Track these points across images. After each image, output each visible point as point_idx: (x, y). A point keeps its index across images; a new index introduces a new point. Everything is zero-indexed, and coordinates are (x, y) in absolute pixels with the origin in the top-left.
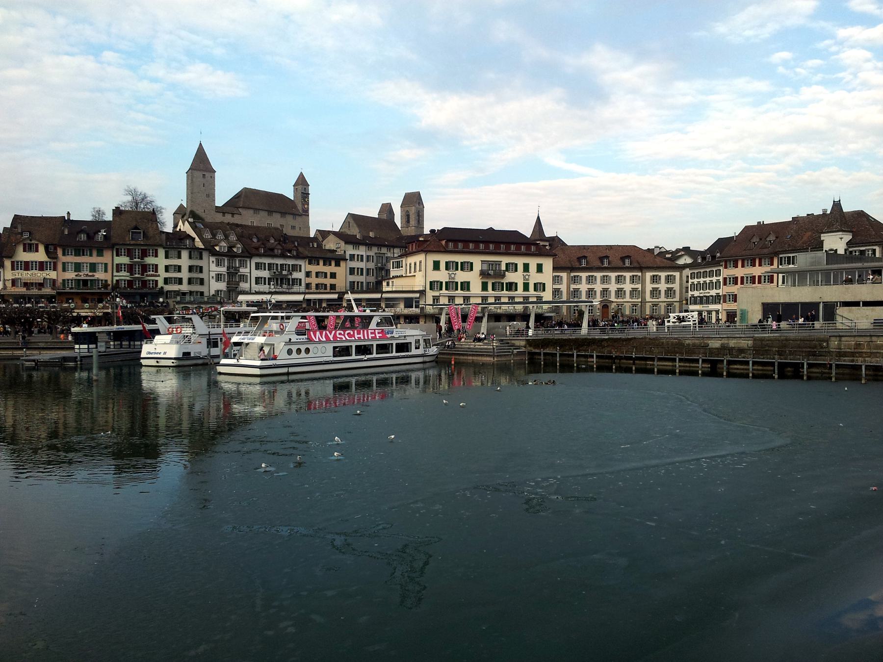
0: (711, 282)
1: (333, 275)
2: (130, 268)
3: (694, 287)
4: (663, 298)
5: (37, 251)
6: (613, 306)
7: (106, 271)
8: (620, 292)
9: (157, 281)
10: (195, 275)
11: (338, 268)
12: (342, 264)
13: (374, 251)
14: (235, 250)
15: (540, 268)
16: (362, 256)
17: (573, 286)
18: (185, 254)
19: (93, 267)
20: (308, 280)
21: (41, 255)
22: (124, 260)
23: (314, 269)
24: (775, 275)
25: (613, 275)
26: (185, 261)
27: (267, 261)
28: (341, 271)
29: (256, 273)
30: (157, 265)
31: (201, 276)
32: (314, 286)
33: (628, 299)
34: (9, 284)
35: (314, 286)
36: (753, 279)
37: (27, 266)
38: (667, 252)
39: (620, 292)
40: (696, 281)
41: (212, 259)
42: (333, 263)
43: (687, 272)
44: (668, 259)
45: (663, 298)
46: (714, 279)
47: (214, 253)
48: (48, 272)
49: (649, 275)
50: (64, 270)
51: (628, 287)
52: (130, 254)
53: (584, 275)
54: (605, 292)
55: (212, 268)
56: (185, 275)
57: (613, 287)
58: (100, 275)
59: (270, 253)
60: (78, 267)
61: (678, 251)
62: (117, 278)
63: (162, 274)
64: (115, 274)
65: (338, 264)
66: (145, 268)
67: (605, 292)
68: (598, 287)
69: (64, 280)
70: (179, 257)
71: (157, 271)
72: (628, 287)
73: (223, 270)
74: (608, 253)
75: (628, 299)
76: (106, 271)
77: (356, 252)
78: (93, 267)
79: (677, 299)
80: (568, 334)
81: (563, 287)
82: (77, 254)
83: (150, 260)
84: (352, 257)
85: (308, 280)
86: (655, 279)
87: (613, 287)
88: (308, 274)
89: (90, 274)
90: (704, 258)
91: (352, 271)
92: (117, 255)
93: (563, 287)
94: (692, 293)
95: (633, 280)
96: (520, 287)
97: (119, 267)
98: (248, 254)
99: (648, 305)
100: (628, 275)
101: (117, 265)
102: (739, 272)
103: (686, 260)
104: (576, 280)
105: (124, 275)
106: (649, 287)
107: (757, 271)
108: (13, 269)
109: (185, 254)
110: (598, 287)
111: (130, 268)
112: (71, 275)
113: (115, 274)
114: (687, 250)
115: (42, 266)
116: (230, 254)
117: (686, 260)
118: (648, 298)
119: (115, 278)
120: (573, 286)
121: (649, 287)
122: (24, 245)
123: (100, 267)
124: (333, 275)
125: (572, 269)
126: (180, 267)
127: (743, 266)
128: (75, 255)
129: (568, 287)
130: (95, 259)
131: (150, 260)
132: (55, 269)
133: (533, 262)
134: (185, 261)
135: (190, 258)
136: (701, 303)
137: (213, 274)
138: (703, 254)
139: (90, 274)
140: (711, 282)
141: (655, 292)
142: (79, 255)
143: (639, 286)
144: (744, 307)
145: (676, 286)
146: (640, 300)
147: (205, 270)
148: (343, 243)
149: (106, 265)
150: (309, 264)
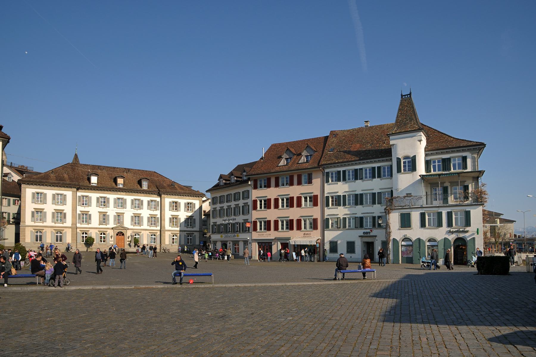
6: (129, 233)
8: (137, 219)
17: (80, 209)
25: (129, 198)
33: (145, 225)
49: (168, 200)
51: (145, 213)
53: (94, 196)
54: (119, 217)
57: (128, 213)
67: (119, 217)
68: (112, 211)
72: (145, 213)
75: (145, 225)
79: (197, 228)
81: (68, 209)
87: (128, 213)
93: (68, 209)
94: (214, 220)
100: (145, 199)
110: (112, 211)
118: (167, 225)
120: (80, 209)
121: (168, 214)
129: (74, 209)
136: (226, 231)
146: (159, 228)
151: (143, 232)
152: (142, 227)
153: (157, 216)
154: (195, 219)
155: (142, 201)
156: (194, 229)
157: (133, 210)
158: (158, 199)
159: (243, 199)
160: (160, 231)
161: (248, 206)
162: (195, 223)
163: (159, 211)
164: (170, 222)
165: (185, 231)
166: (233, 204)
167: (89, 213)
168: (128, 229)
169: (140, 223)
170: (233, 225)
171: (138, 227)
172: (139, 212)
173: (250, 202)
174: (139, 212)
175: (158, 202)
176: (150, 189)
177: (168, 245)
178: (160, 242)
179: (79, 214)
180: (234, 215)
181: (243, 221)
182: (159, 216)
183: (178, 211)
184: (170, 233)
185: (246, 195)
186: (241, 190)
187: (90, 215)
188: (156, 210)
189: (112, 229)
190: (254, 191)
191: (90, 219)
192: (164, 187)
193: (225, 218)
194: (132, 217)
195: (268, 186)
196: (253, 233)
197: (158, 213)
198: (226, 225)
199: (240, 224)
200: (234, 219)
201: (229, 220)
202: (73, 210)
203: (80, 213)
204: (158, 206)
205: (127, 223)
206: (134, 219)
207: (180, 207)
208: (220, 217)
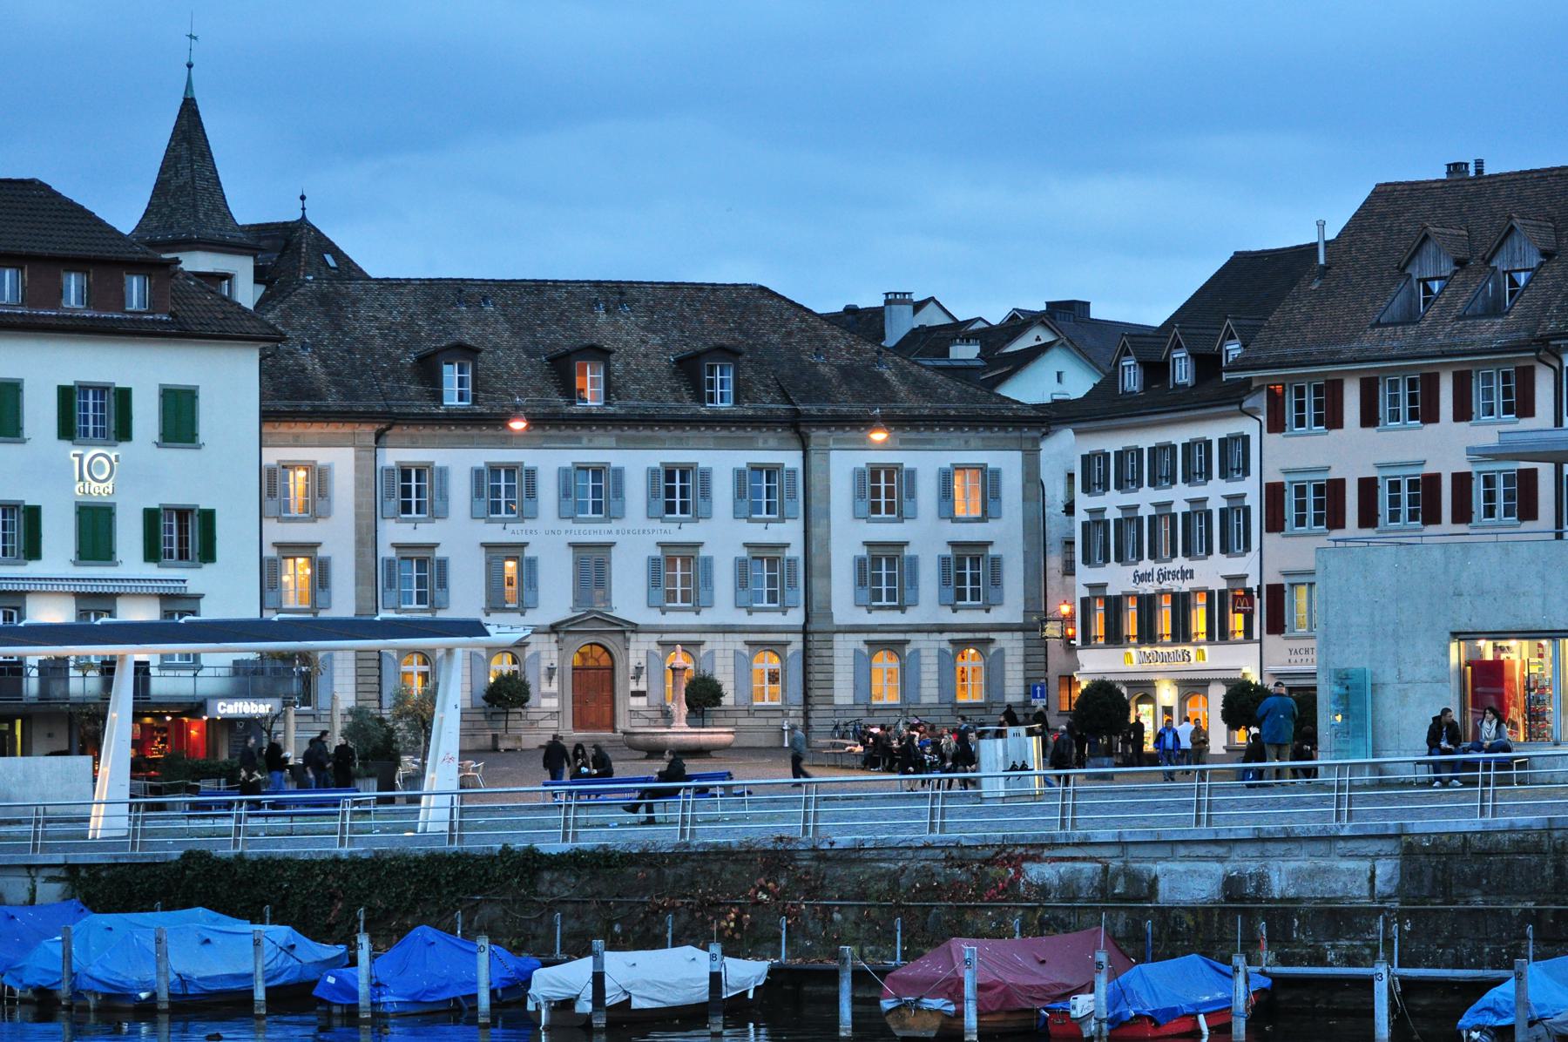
0: (1199, 512)
3: (1106, 539)
4: (928, 606)
6: (638, 651)
8: (679, 571)
15: (180, 417)
17: (395, 532)
24: (1546, 472)
25: (637, 463)
33: (724, 609)
36: (1424, 497)
38: (958, 330)
39: (679, 571)
40: (1112, 503)
43: (1064, 449)
44: (960, 372)
45: (928, 606)
46: (1215, 493)
49: (843, 464)
51: (723, 535)
57: (636, 537)
61: (1018, 323)
67: (592, 565)
72: (723, 535)
74: (602, 326)
75: (724, 609)
79: (1011, 609)
80: (346, 829)
86: (884, 492)
87: (636, 537)
90: (1156, 371)
95: (759, 495)
96: (59, 535)
99: (845, 649)
100: (723, 464)
102: (1351, 451)
103: (1057, 378)
104: (413, 492)
106: (848, 536)
107: (1446, 446)
110: (549, 537)
114: (1067, 317)
117: (1057, 378)
118: (844, 604)
120: (395, 532)
121: (848, 536)
125: (388, 421)
127: (1369, 418)
129: (367, 539)
133: (144, 371)
138: (1133, 338)
140: (1199, 512)
141: (884, 570)
143: (789, 533)
144: (1354, 659)
145: (1005, 536)
146: (796, 617)
151: (712, 642)
152: (707, 618)
153: (788, 553)
154: (996, 562)
155: (706, 475)
156: (997, 616)
157: (657, 524)
158: (791, 459)
159: (1224, 474)
160: (805, 631)
161: (1247, 510)
162: (996, 580)
163: (798, 525)
164: (861, 582)
165: (941, 629)
166: (1179, 496)
167: (439, 553)
168: (636, 629)
169: (696, 593)
170: (1182, 604)
171: (689, 619)
172: (687, 532)
173: (1250, 489)
174: (687, 532)
175: (793, 472)
176: (747, 410)
177: (846, 708)
178: (806, 696)
179: (390, 562)
180: (1188, 552)
181: (1223, 585)
182: (796, 551)
183: (901, 518)
184: (856, 641)
185: (1235, 457)
186: (1214, 431)
187: (443, 564)
188: (782, 519)
189: (554, 629)
190: (1273, 439)
191: (443, 583)
192: (819, 390)
193: (1146, 565)
194: (654, 563)
195: (1331, 418)
196: (1271, 641)
197: (789, 533)
198: (1147, 605)
199: (1210, 594)
200: (1187, 574)
201: (1163, 576)
202: (360, 542)
203: (392, 553)
204: (793, 496)
205: (628, 597)
206: (665, 573)
207: (912, 495)
208: (1120, 558)
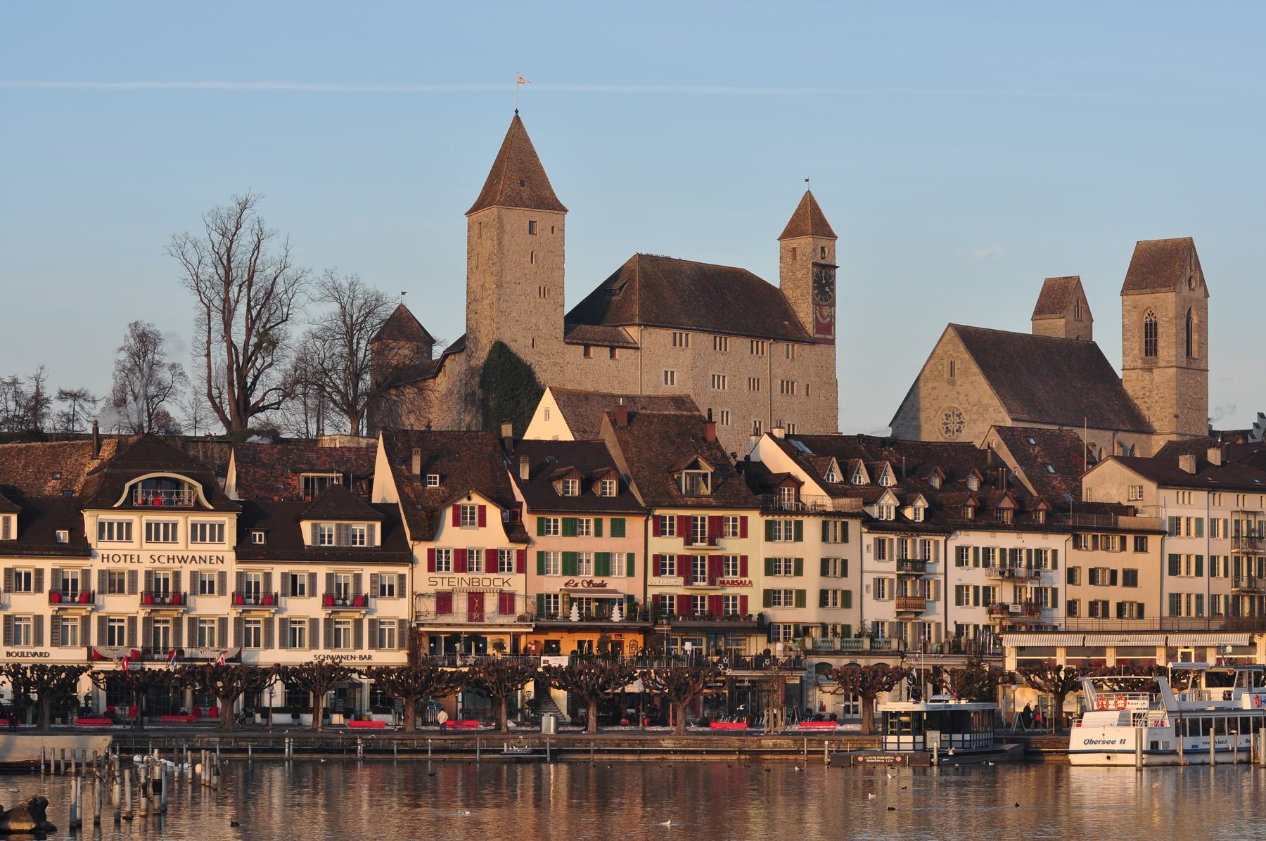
1: (1131, 578)
2: (686, 567)
5: (483, 523)
7: (631, 572)
9: (744, 599)
10: (831, 583)
11: (1140, 556)
12: (1153, 542)
13: (1227, 505)
14: (909, 513)
16: (1199, 521)
18: (812, 527)
19: (604, 563)
20: (1073, 592)
21: (493, 535)
22: (673, 545)
23: (1086, 559)
26: (811, 547)
27: (978, 539)
28: (1148, 564)
29: (958, 575)
30: (744, 559)
31: (844, 584)
32: (1084, 609)
34: (430, 605)
35: (1084, 609)
37: (463, 560)
41: (869, 539)
42: (1130, 540)
47: (872, 524)
48: (505, 575)
50: (542, 570)
52: (687, 530)
55: (870, 562)
56: (811, 582)
58: (619, 583)
59: (986, 520)
60: (571, 563)
62: (656, 591)
63: (759, 581)
64: (652, 579)
65: (1141, 547)
66: (718, 564)
69: (540, 597)
70: (799, 537)
71: (744, 573)
73: (889, 568)
76: (631, 572)
77: (1181, 512)
78: (604, 563)
82: (571, 529)
83: (731, 546)
84: (1176, 521)
85: (1073, 592)
88: (1071, 576)
89: (598, 580)
91: (1174, 565)
92: (656, 534)
97: (660, 564)
98: (942, 521)
101: (655, 557)
105: (671, 585)
108: (431, 568)
109: (812, 527)
111: (686, 567)
112: (554, 583)
113: (652, 579)
115: (495, 561)
116: (901, 525)
119: (652, 592)
122: (456, 509)
123: (619, 564)
124: (1131, 578)
126: (799, 562)
128: (565, 534)
130: (607, 543)
131: (731, 546)
132: (522, 568)
134: (811, 547)
135: (825, 538)
137: (869, 580)
139: (598, 580)
142: (574, 534)
147: (853, 568)
148: (1150, 487)
149: (631, 557)
150: (1077, 546)
